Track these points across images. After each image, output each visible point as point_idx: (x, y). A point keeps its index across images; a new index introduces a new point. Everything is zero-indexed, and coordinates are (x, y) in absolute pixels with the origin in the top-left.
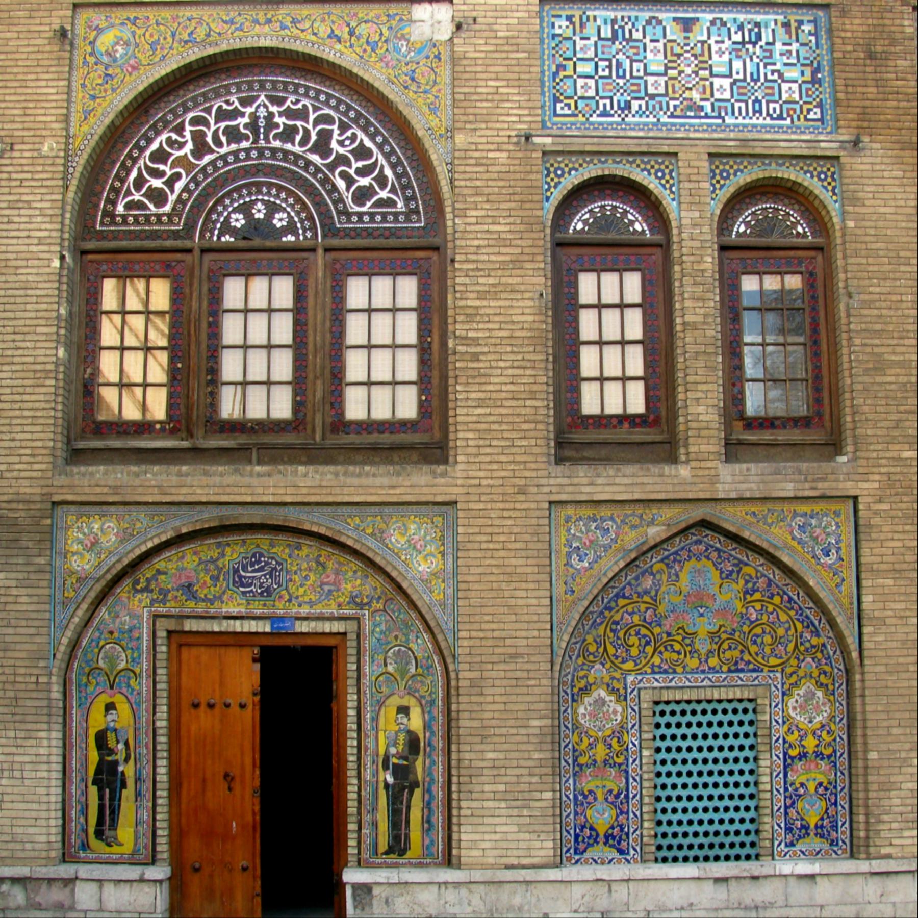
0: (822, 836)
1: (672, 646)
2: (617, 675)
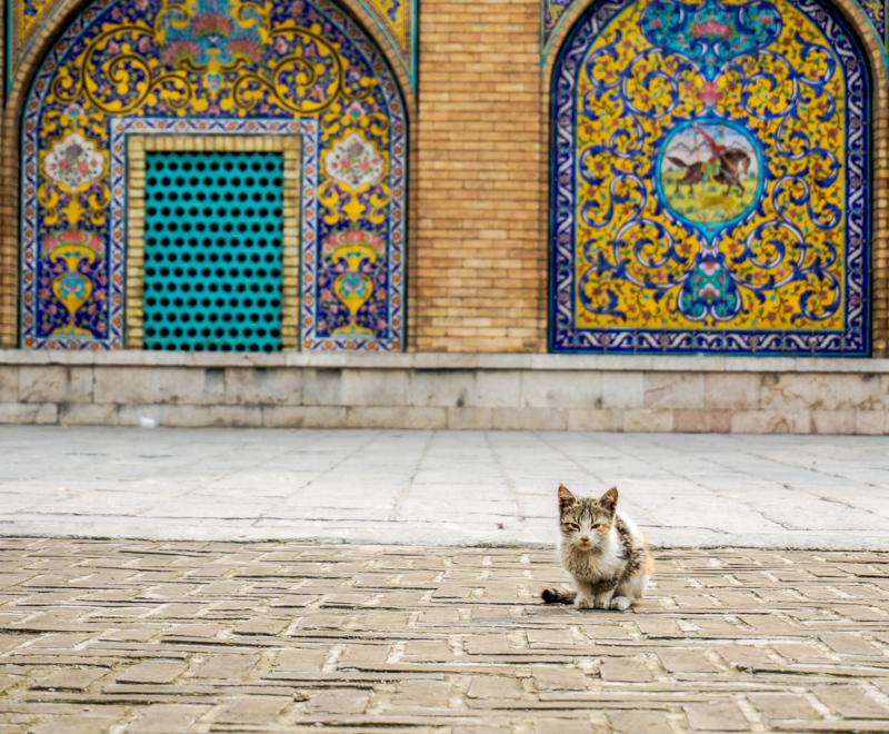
0: (366, 325)
1: (172, 83)
2: (99, 117)
